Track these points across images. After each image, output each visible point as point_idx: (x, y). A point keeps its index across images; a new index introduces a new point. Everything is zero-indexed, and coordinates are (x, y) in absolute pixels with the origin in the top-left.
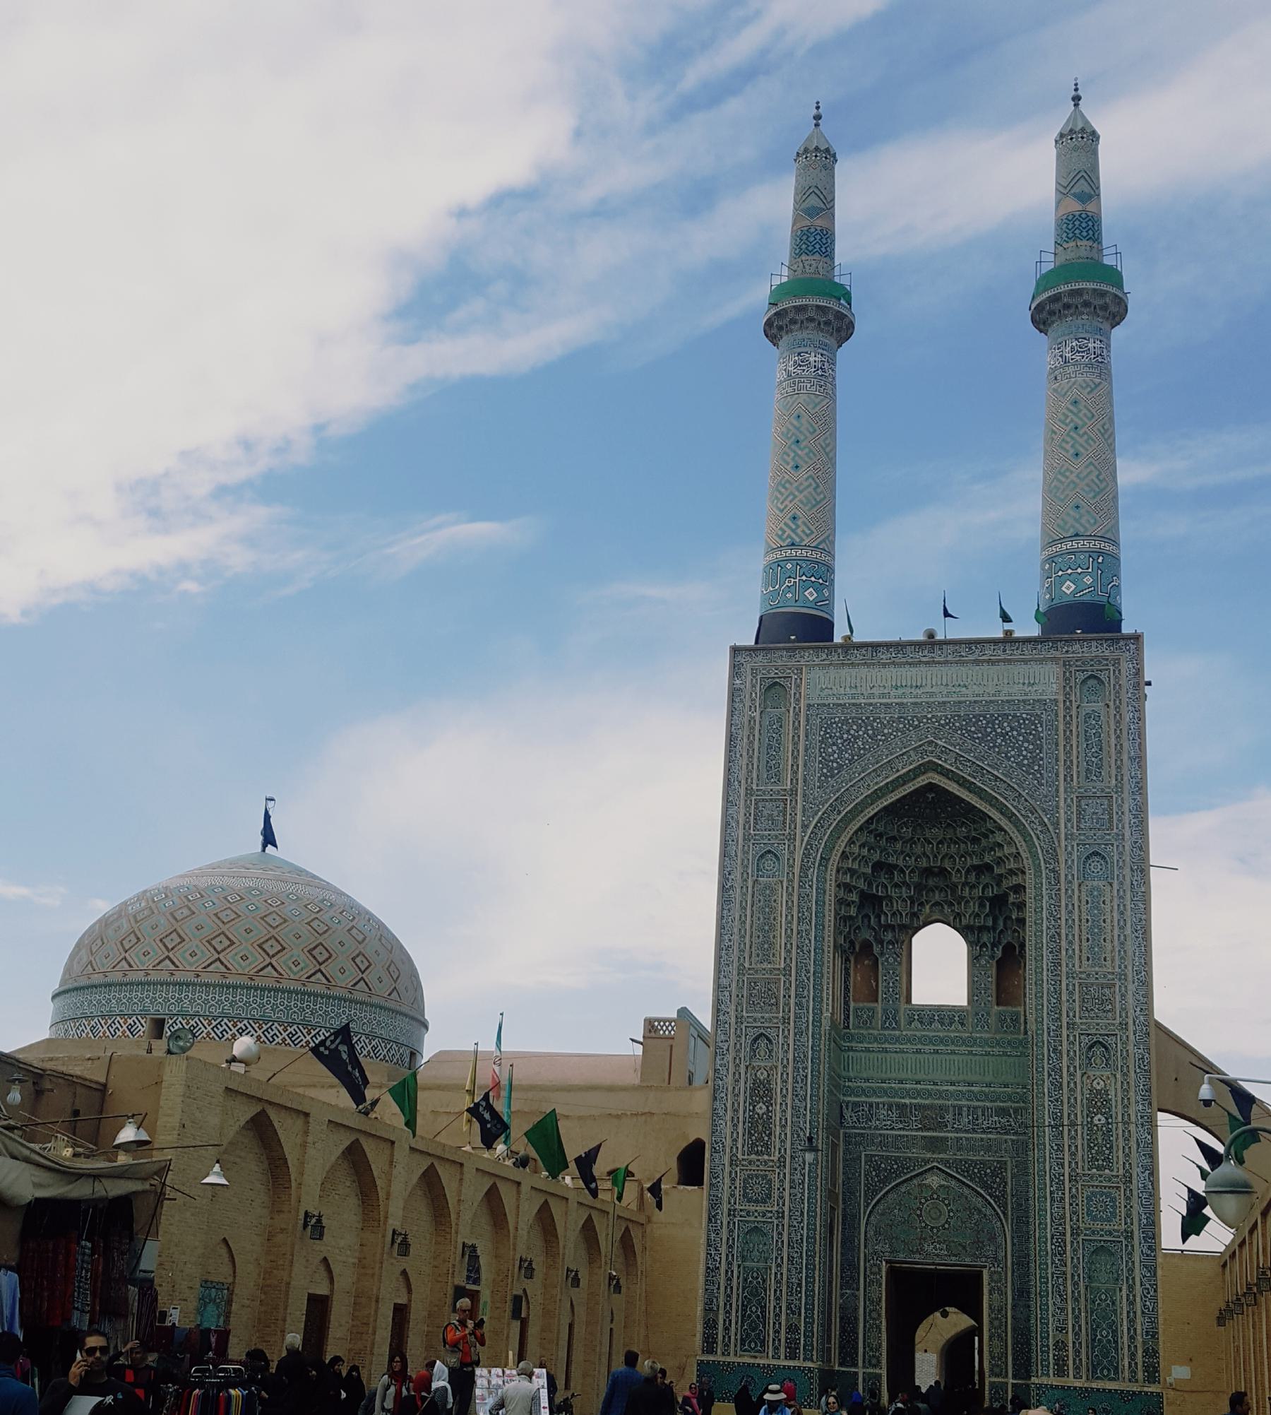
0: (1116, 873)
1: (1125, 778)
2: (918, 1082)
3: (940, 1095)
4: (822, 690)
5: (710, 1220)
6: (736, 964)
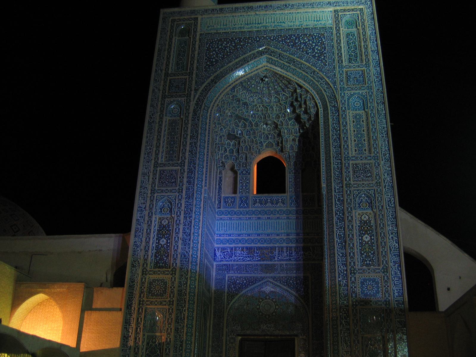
0: (369, 105)
1: (371, 61)
2: (259, 235)
3: (271, 241)
4: (208, 27)
5: (127, 307)
6: (153, 161)
